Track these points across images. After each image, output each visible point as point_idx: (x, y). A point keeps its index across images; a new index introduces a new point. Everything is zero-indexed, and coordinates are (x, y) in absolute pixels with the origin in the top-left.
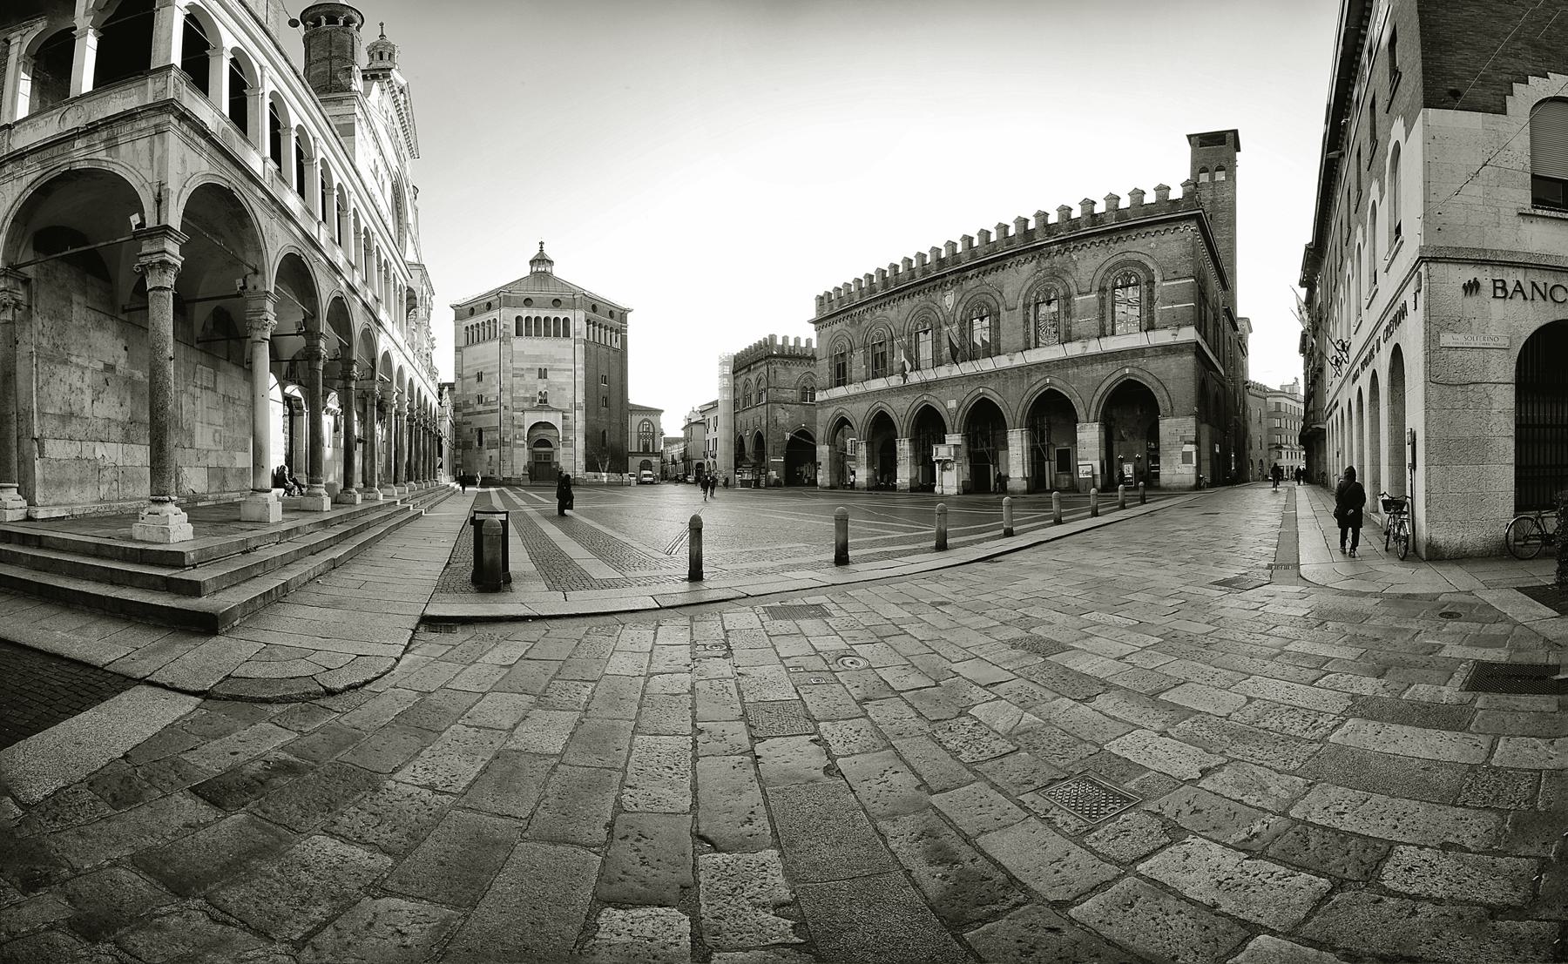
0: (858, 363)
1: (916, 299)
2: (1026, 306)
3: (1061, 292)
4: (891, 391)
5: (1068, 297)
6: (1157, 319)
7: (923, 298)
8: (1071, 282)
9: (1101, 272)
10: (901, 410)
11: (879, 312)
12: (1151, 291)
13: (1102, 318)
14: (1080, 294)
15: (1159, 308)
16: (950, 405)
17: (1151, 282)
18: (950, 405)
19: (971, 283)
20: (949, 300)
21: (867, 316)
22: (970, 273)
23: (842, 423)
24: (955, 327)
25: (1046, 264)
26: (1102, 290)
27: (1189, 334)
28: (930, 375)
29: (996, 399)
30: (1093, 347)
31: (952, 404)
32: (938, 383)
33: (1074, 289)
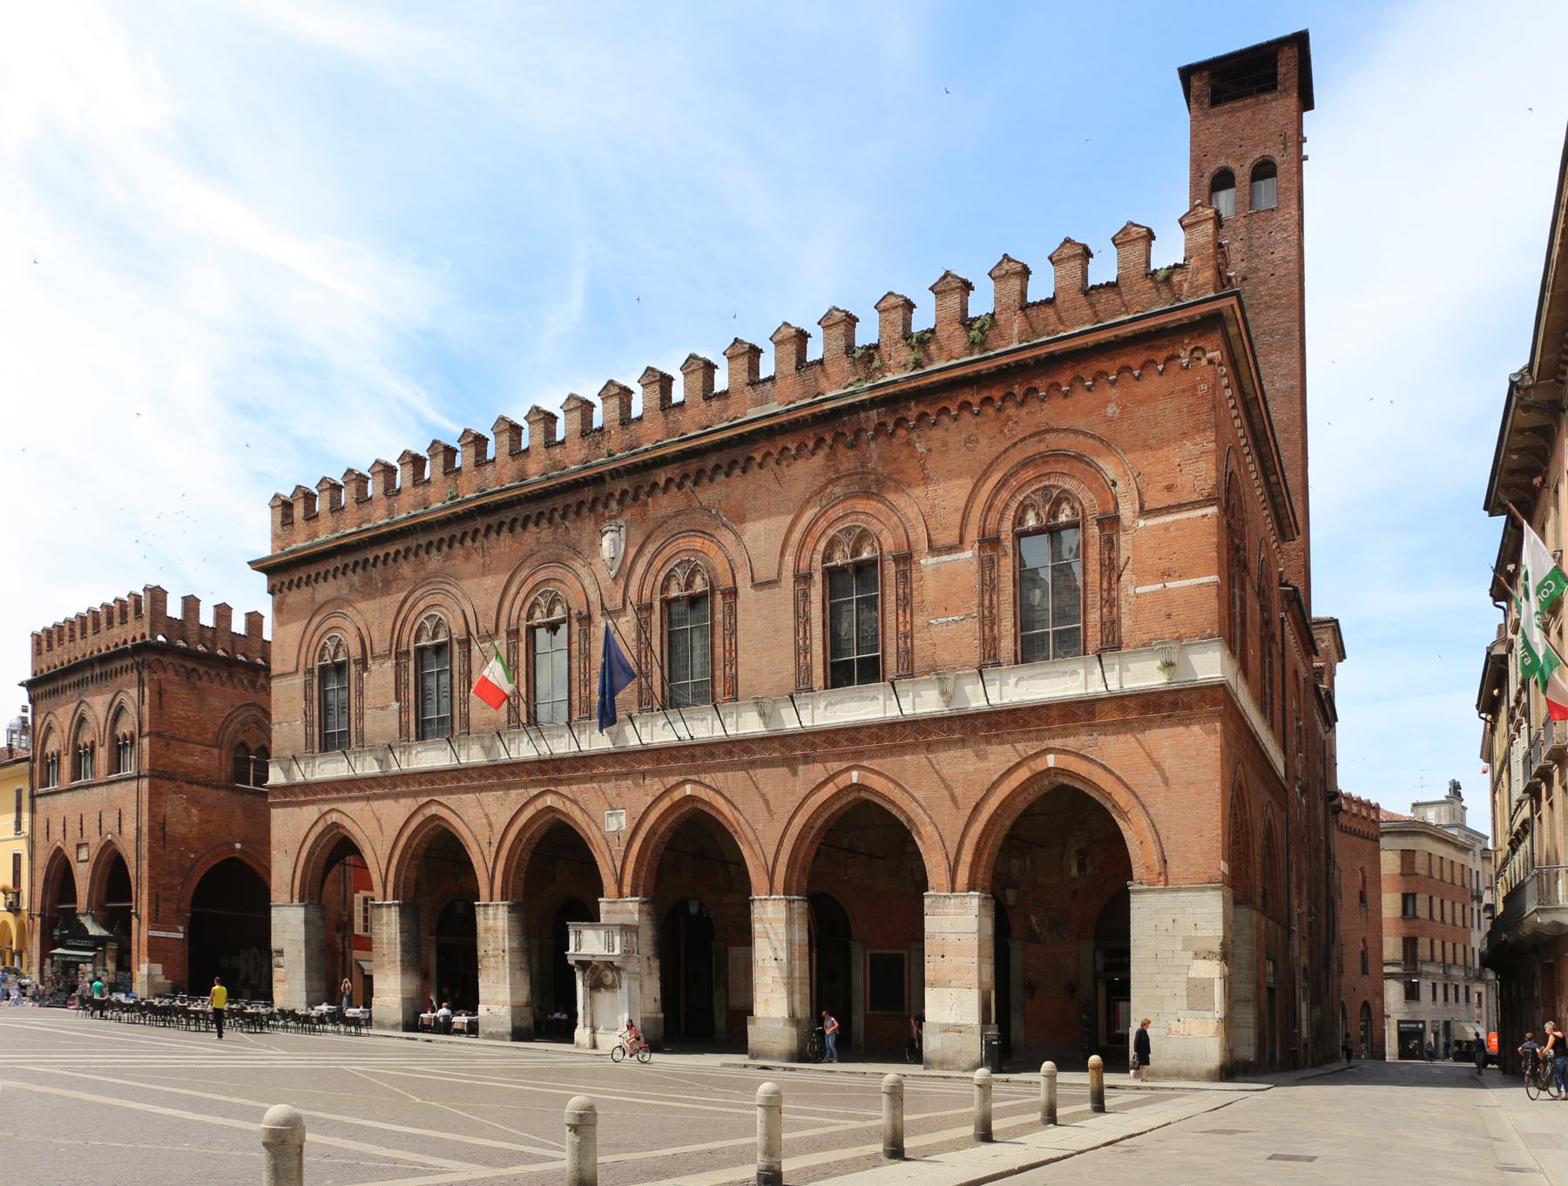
0: (379, 698)
2: (803, 578)
5: (905, 559)
6: (1126, 621)
7: (546, 533)
8: (911, 512)
12: (1110, 544)
14: (934, 550)
15: (1135, 589)
16: (613, 822)
18: (613, 822)
22: (661, 476)
23: (336, 856)
24: (626, 625)
25: (848, 460)
26: (989, 542)
28: (562, 746)
31: (617, 823)
33: (919, 536)
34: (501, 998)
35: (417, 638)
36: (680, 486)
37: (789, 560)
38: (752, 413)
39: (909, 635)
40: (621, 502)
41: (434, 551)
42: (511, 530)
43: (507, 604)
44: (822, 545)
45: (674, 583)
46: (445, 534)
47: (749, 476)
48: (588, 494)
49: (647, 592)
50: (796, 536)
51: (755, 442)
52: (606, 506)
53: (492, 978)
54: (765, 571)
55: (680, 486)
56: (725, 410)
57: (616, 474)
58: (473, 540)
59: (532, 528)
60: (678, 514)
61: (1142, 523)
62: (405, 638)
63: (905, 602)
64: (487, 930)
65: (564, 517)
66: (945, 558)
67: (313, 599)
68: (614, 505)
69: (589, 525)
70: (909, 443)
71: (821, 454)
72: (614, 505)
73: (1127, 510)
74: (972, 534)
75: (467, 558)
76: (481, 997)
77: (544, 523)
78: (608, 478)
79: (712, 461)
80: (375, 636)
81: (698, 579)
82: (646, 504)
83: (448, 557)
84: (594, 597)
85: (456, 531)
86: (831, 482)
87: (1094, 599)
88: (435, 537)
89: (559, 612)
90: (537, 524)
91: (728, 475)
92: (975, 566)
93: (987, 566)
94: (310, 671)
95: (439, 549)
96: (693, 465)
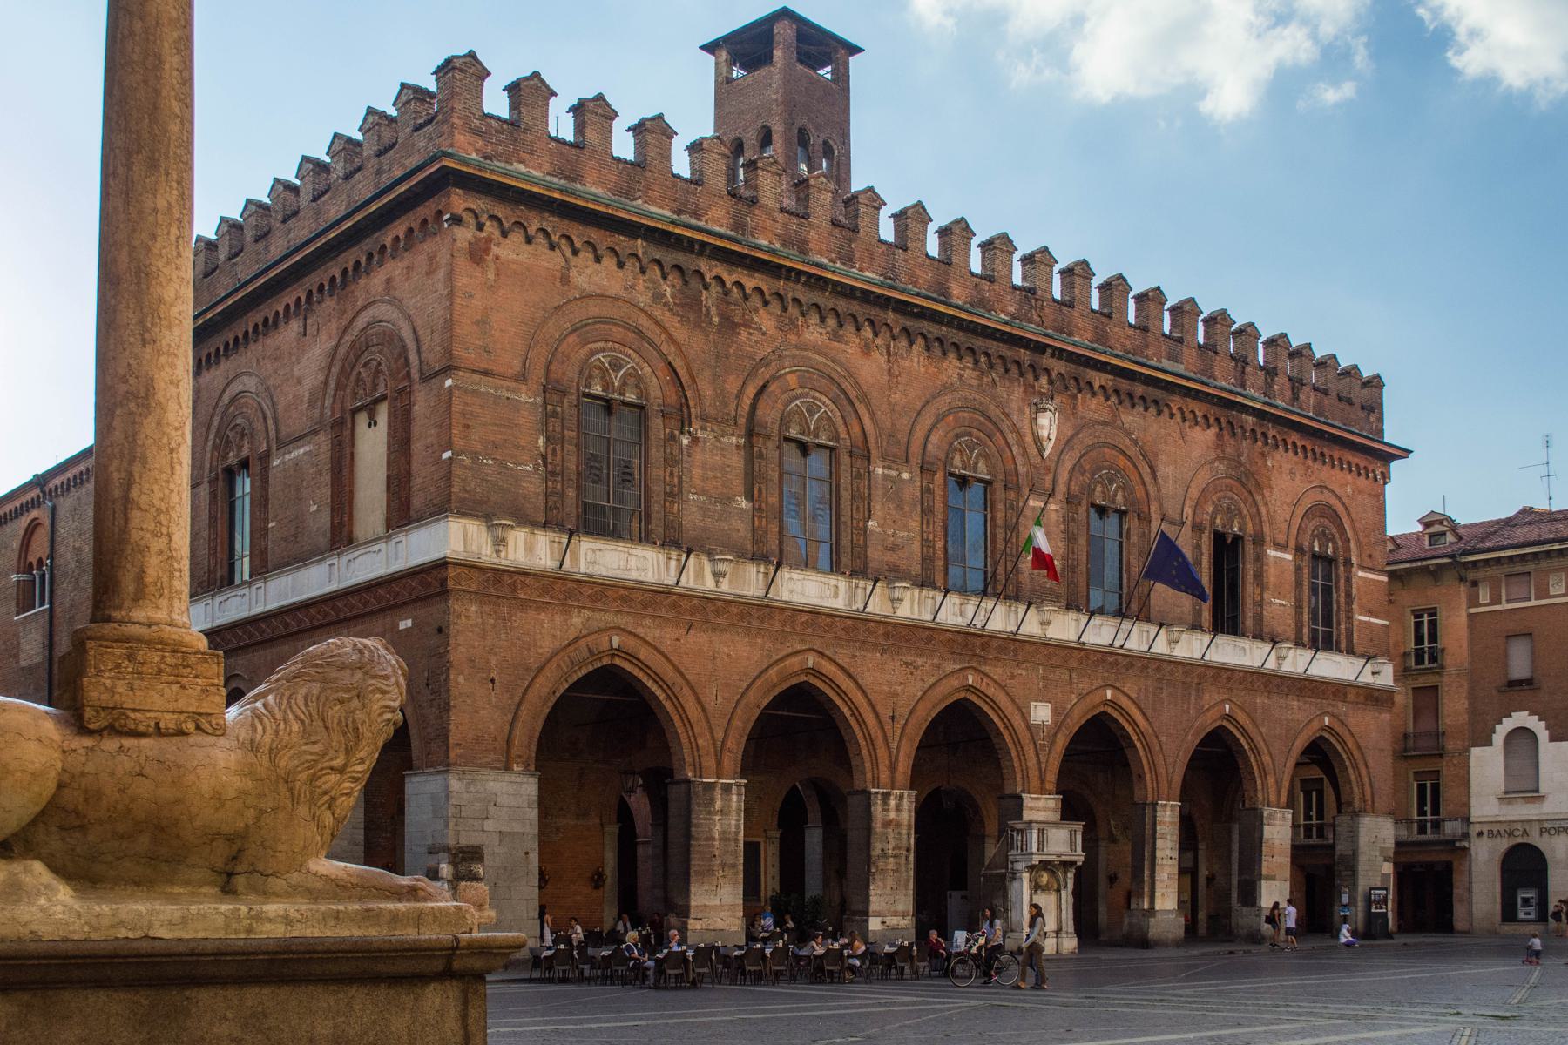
1: (952, 368)
3: (1250, 529)
4: (854, 627)
5: (1259, 541)
8: (1263, 510)
9: (1300, 513)
10: (890, 702)
11: (814, 333)
12: (1348, 579)
13: (1298, 608)
14: (1279, 546)
17: (1348, 563)
19: (1093, 407)
20: (1048, 425)
21: (766, 320)
22: (1098, 379)
25: (1230, 444)
26: (1299, 550)
27: (1384, 675)
29: (1137, 722)
30: (1297, 661)
31: (1041, 713)
32: (1012, 645)
33: (1266, 528)
34: (900, 907)
35: (784, 422)
36: (1107, 399)
37: (1188, 511)
38: (1166, 364)
39: (1260, 604)
40: (1051, 382)
41: (814, 318)
42: (928, 349)
43: (919, 434)
44: (1210, 509)
45: (1099, 488)
46: (842, 305)
47: (1161, 418)
48: (1025, 355)
49: (1075, 488)
50: (1194, 492)
51: (1173, 393)
52: (1037, 379)
53: (890, 882)
54: (1172, 513)
55: (1107, 399)
56: (1146, 346)
57: (1059, 353)
58: (876, 334)
59: (952, 356)
60: (1105, 423)
61: (1360, 574)
62: (759, 412)
63: (1259, 576)
64: (887, 824)
65: (991, 366)
66: (1279, 554)
67: (565, 279)
68: (1044, 380)
69: (1018, 392)
70: (1263, 454)
71: (1213, 431)
72: (1044, 380)
73: (1354, 560)
74: (1292, 544)
75: (866, 349)
76: (873, 907)
77: (968, 361)
78: (1049, 351)
79: (1139, 389)
80: (707, 391)
81: (1119, 497)
82: (1075, 397)
83: (835, 337)
84: (1021, 469)
85: (855, 307)
86: (1218, 458)
87: (1343, 615)
88: (826, 301)
89: (982, 471)
90: (960, 358)
91: (1146, 409)
92: (1292, 568)
93: (1298, 569)
94: (551, 389)
95: (823, 319)
96: (1124, 384)
